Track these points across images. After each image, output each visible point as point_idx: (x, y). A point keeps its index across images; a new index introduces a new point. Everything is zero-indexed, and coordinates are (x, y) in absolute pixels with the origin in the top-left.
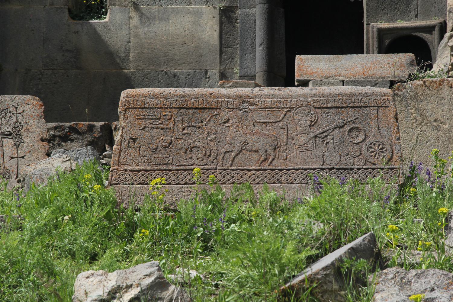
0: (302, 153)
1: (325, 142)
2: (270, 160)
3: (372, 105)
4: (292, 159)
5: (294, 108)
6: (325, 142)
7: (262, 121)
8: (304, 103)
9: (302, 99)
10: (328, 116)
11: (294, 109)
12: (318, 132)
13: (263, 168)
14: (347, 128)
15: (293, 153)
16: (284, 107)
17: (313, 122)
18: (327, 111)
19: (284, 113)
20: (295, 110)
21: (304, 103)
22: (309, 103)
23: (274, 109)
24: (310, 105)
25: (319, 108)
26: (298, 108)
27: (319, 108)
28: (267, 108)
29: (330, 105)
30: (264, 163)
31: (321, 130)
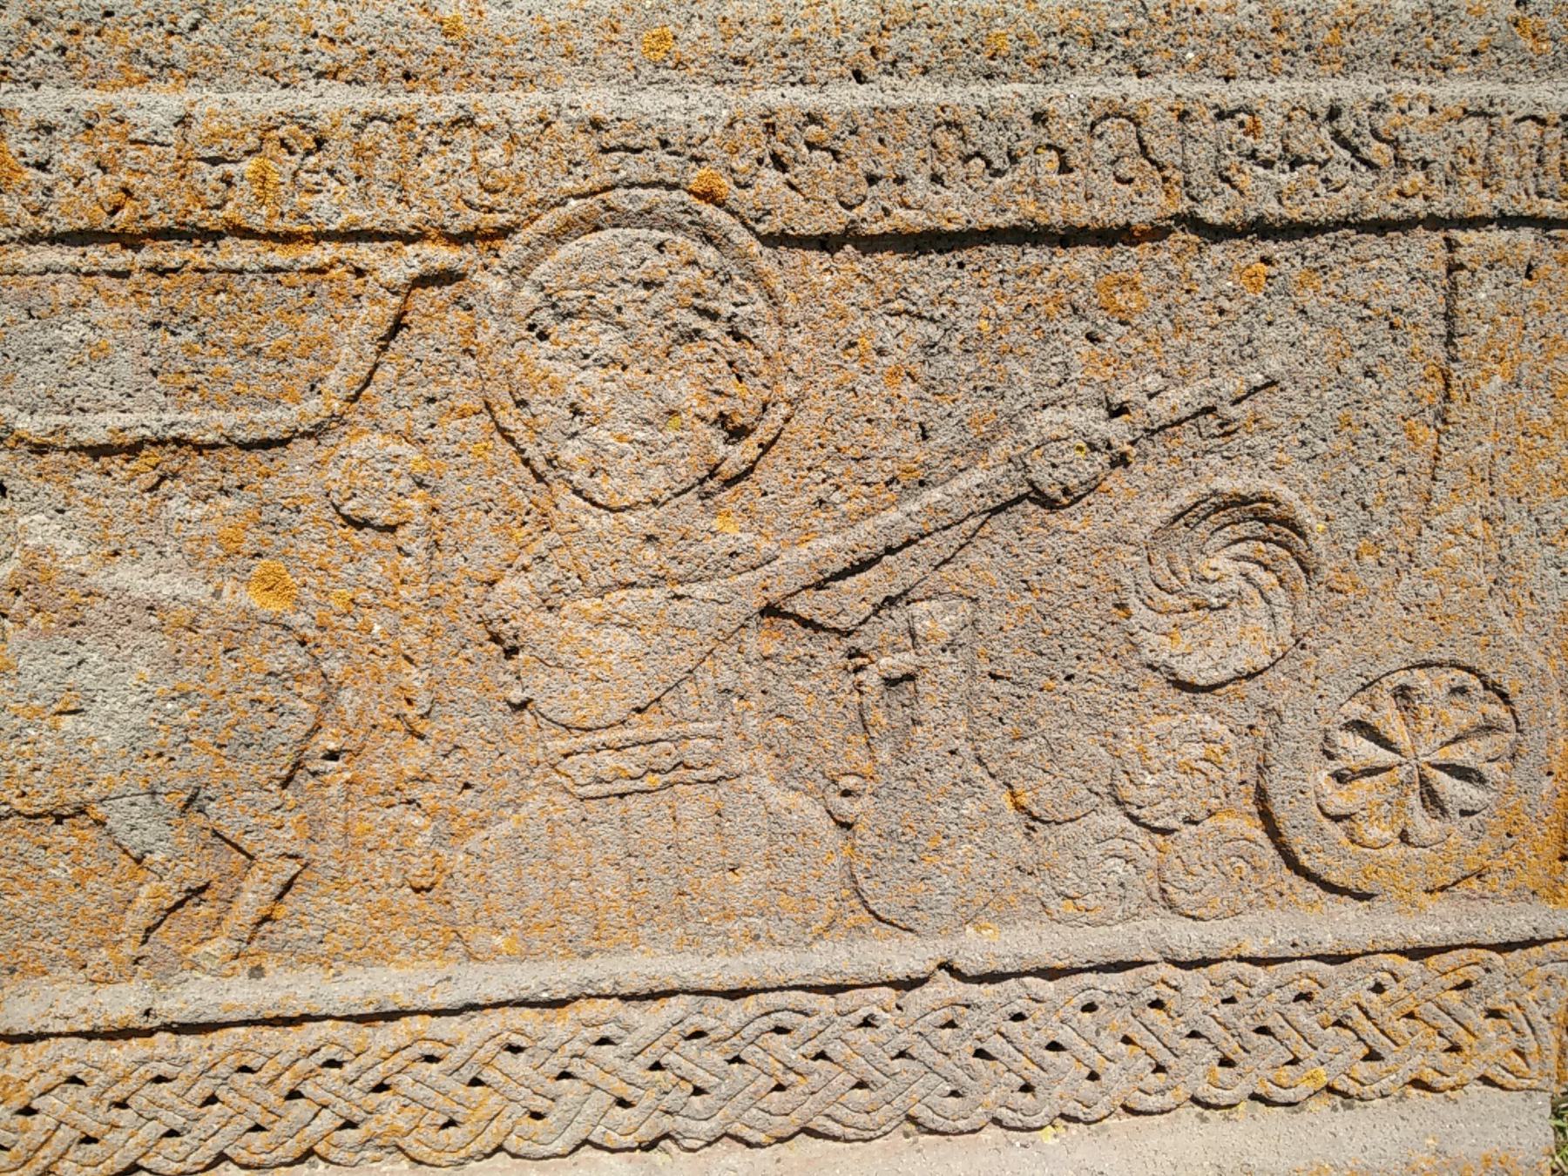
0: (618, 806)
1: (871, 678)
2: (253, 897)
3: (1484, 202)
4: (501, 876)
5: (504, 232)
6: (871, 678)
7: (96, 429)
8: (634, 168)
9: (598, 100)
10: (929, 347)
11: (510, 250)
12: (797, 561)
13: (175, 1006)
14: (1143, 501)
15: (515, 804)
16: (366, 217)
17: (738, 434)
18: (927, 275)
19: (381, 313)
20: (518, 272)
21: (634, 168)
22: (696, 176)
23: (235, 253)
24: (708, 196)
25: (826, 243)
26: (558, 236)
27: (826, 243)
28: (132, 241)
29: (958, 207)
30: (176, 923)
31: (831, 546)
